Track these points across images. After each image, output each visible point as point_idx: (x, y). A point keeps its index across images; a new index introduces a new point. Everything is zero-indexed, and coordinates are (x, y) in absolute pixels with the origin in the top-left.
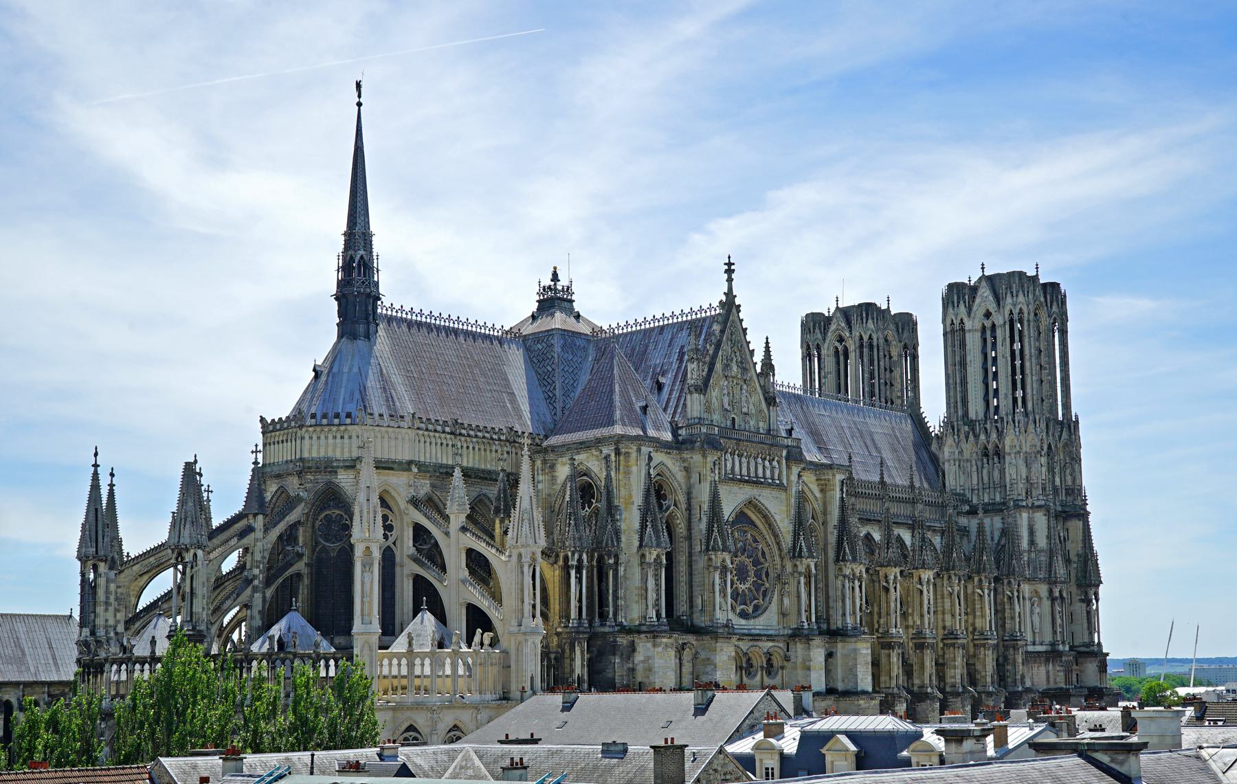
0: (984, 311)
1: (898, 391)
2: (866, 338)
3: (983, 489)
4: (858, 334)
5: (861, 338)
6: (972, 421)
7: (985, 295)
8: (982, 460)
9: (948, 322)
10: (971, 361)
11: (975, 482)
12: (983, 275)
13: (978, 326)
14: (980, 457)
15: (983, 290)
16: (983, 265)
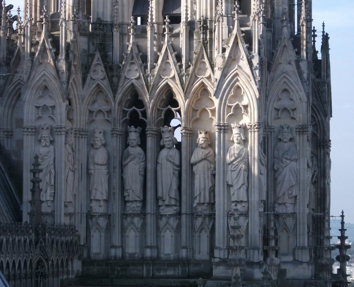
3: (124, 216)
6: (99, 24)
8: (126, 135)
14: (119, 128)
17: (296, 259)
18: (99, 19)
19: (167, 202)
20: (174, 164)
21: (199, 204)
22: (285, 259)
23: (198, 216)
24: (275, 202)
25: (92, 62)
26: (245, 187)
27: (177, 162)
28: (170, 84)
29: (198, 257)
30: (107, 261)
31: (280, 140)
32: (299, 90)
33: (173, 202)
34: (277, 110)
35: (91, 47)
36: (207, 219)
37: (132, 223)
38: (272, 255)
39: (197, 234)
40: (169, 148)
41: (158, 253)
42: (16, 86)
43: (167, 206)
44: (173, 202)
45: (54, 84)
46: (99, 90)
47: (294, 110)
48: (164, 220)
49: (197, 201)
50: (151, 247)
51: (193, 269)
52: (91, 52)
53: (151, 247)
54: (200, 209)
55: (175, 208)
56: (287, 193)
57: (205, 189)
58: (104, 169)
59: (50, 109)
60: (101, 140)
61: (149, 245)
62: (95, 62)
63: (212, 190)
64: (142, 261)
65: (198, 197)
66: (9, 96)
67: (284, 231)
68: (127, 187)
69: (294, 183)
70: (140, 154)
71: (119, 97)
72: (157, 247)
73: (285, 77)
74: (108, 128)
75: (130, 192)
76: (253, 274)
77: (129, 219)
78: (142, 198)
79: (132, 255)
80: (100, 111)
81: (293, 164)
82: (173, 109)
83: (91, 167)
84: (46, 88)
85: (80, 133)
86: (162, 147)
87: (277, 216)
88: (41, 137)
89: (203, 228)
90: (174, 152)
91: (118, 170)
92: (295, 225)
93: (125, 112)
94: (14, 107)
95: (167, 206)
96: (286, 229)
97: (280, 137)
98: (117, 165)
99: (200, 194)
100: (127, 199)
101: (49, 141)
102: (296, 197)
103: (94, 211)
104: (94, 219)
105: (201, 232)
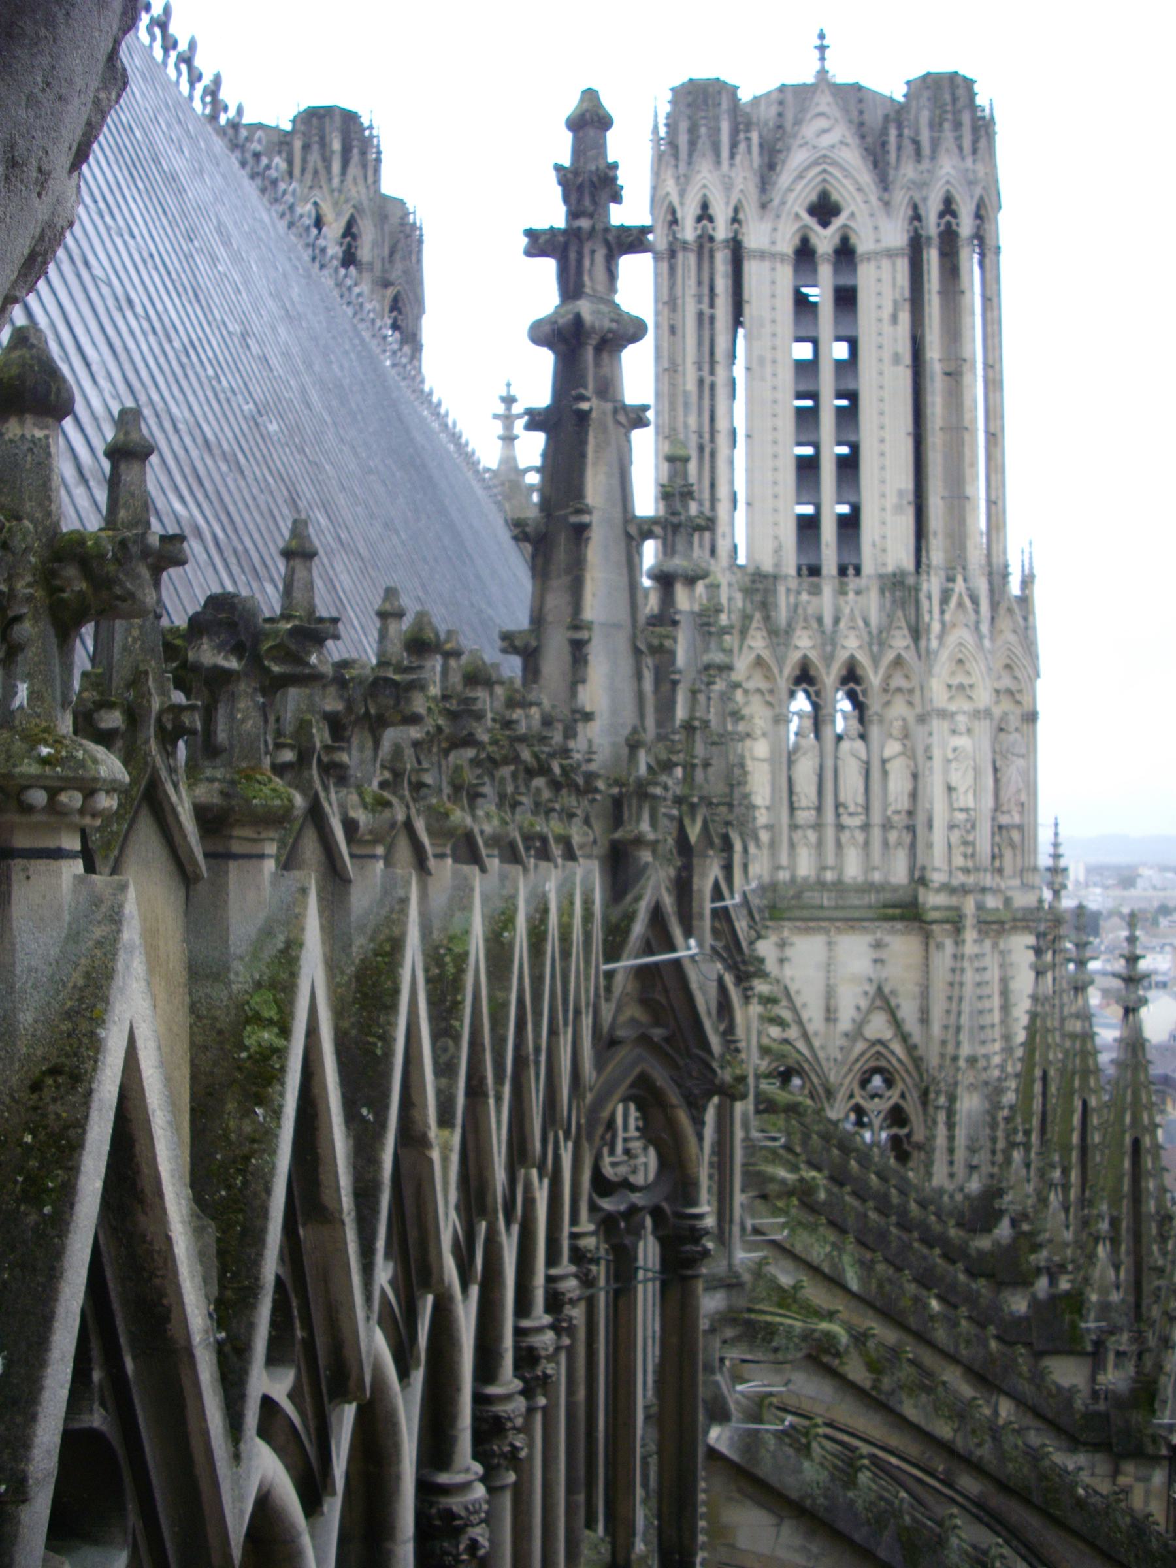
0: (814, 197)
3: (794, 827)
7: (826, 141)
12: (823, 72)
13: (787, 245)
15: (822, 123)
16: (822, 36)
19: (852, 809)
20: (859, 759)
23: (892, 827)
27: (864, 756)
31: (1001, 730)
33: (860, 810)
35: (749, 606)
37: (805, 837)
41: (841, 873)
46: (759, 662)
53: (832, 868)
58: (766, 767)
62: (754, 624)
64: (822, 885)
68: (798, 788)
71: (787, 671)
77: (800, 833)
79: (806, 879)
81: (1021, 762)
87: (1000, 827)
95: (851, 814)
96: (1012, 845)
102: (1023, 805)
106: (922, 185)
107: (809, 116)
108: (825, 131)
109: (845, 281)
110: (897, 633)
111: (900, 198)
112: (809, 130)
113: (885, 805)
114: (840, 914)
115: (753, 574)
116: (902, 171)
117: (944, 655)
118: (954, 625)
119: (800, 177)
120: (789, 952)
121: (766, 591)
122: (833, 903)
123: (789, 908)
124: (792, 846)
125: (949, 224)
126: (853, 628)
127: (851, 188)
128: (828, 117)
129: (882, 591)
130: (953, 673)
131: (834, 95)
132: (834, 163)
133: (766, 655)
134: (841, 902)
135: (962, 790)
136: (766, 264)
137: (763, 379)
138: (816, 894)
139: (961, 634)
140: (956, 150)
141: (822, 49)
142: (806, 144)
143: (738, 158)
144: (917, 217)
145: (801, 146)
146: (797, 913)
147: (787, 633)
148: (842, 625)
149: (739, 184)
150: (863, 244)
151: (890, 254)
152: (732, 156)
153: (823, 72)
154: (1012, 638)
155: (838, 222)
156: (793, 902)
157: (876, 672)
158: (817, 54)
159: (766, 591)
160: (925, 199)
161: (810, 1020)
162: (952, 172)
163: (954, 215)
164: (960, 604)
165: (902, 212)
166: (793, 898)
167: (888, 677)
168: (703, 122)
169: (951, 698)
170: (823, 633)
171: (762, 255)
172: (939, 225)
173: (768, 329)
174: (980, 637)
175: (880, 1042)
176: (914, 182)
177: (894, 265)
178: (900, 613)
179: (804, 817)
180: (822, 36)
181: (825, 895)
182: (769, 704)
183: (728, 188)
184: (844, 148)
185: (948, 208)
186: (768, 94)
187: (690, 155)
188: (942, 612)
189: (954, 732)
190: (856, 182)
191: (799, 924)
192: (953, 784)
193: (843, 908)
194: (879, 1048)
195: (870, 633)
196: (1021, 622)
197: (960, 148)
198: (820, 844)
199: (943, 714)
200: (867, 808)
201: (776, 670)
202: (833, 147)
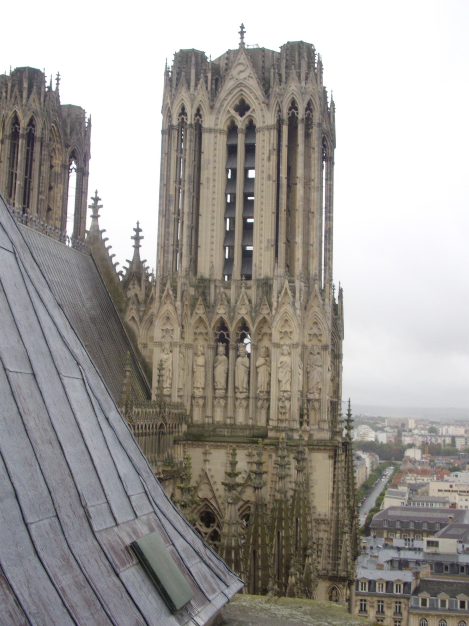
0: (237, 102)
1: (56, 219)
2: (24, 123)
3: (215, 398)
4: (11, 114)
5: (16, 121)
6: (202, 280)
7: (243, 76)
8: (217, 347)
9: (176, 111)
10: (208, 179)
11: (200, 382)
12: (242, 44)
13: (223, 125)
14: (212, 343)
15: (241, 68)
16: (242, 27)
17: (320, 427)
18: (201, 276)
19: (241, 390)
20: (245, 366)
21: (261, 392)
22: (313, 427)
23: (260, 399)
24: (307, 392)
25: (197, 302)
26: (289, 382)
27: (248, 365)
28: (245, 317)
29: (259, 424)
30: (203, 426)
31: (311, 353)
32: (323, 322)
33: (245, 390)
34: (310, 335)
35: (197, 293)
36: (265, 401)
37: (219, 402)
38: (305, 425)
39: (259, 411)
40: (243, 357)
41: (235, 421)
42: (150, 316)
43: (241, 392)
44: (245, 390)
45: (173, 316)
46: (201, 320)
47: (320, 335)
48: (239, 401)
49: (259, 390)
50: (230, 418)
51: (256, 432)
52: (196, 297)
53: (230, 418)
54: (261, 394)
55: (246, 394)
56: (315, 387)
57: (264, 382)
58: (202, 369)
59: (171, 331)
60: (201, 351)
61: (229, 416)
62: (199, 302)
63: (269, 384)
65: (260, 388)
66: (146, 322)
67: (313, 410)
68: (216, 380)
69: (319, 380)
70: (225, 360)
71: (213, 324)
72: (234, 418)
73: (315, 315)
74: (205, 344)
75: (219, 383)
76: (293, 437)
77: (217, 400)
78: (225, 387)
79: (218, 422)
80: (201, 333)
81: (320, 369)
82: (246, 333)
83: (195, 367)
84: (168, 318)
85: (188, 346)
86: (238, 356)
87: (309, 401)
88: (165, 348)
89: (263, 407)
90: (246, 360)
91: (211, 370)
92: (320, 406)
93: (216, 334)
94: (148, 329)
95: (241, 392)
96: (314, 409)
97: (312, 352)
98: (211, 366)
99: (261, 386)
100: (216, 387)
101: (169, 351)
102: (320, 389)
103: (196, 394)
104: (196, 399)
105: (261, 409)
106: (281, 95)
107: (235, 65)
108: (242, 72)
109: (249, 141)
110: (264, 307)
111: (273, 101)
112: (234, 72)
113: (257, 388)
114: (232, 440)
115: (199, 279)
116: (275, 89)
117: (278, 318)
118: (283, 303)
119: (230, 93)
120: (208, 457)
121: (205, 287)
122: (230, 434)
123: (209, 436)
124: (213, 407)
125: (293, 113)
126: (243, 304)
127: (253, 98)
128: (244, 65)
129: (258, 287)
130: (283, 326)
131: (246, 55)
132: (245, 87)
133: (204, 317)
134: (233, 434)
135: (284, 382)
136: (213, 135)
137: (208, 188)
138: (222, 430)
139: (288, 308)
140: (297, 78)
141: (242, 33)
142: (233, 78)
143: (199, 86)
144: (280, 111)
145: (231, 79)
146: (212, 439)
147: (213, 306)
148: (238, 303)
149: (199, 98)
150: (258, 124)
151: (269, 128)
152: (196, 85)
153: (242, 44)
154: (316, 309)
155: (248, 114)
156: (212, 433)
157: (253, 326)
158: (239, 36)
159: (205, 287)
160: (282, 102)
161: (217, 490)
162: (295, 89)
163: (296, 109)
164: (286, 293)
165: (274, 108)
166: (212, 431)
167: (260, 328)
168: (183, 70)
169: (281, 338)
170: (230, 306)
171: (210, 130)
172: (289, 114)
173: (211, 165)
174: (295, 309)
175: (206, 499)
176: (279, 94)
177: (270, 133)
178: (265, 298)
179: (220, 393)
180: (242, 27)
181: (226, 430)
182: (206, 339)
183: (193, 100)
184: (250, 79)
185: (293, 106)
186: (223, 55)
187: (177, 85)
188: (278, 297)
189: (282, 354)
190: (256, 95)
191: (213, 443)
192: (280, 379)
193: (234, 437)
194: (207, 502)
195: (251, 307)
196: (321, 302)
197: (299, 77)
198: (226, 406)
199: (278, 346)
200: (249, 390)
201: (208, 324)
202: (245, 79)
